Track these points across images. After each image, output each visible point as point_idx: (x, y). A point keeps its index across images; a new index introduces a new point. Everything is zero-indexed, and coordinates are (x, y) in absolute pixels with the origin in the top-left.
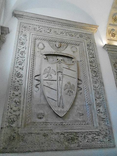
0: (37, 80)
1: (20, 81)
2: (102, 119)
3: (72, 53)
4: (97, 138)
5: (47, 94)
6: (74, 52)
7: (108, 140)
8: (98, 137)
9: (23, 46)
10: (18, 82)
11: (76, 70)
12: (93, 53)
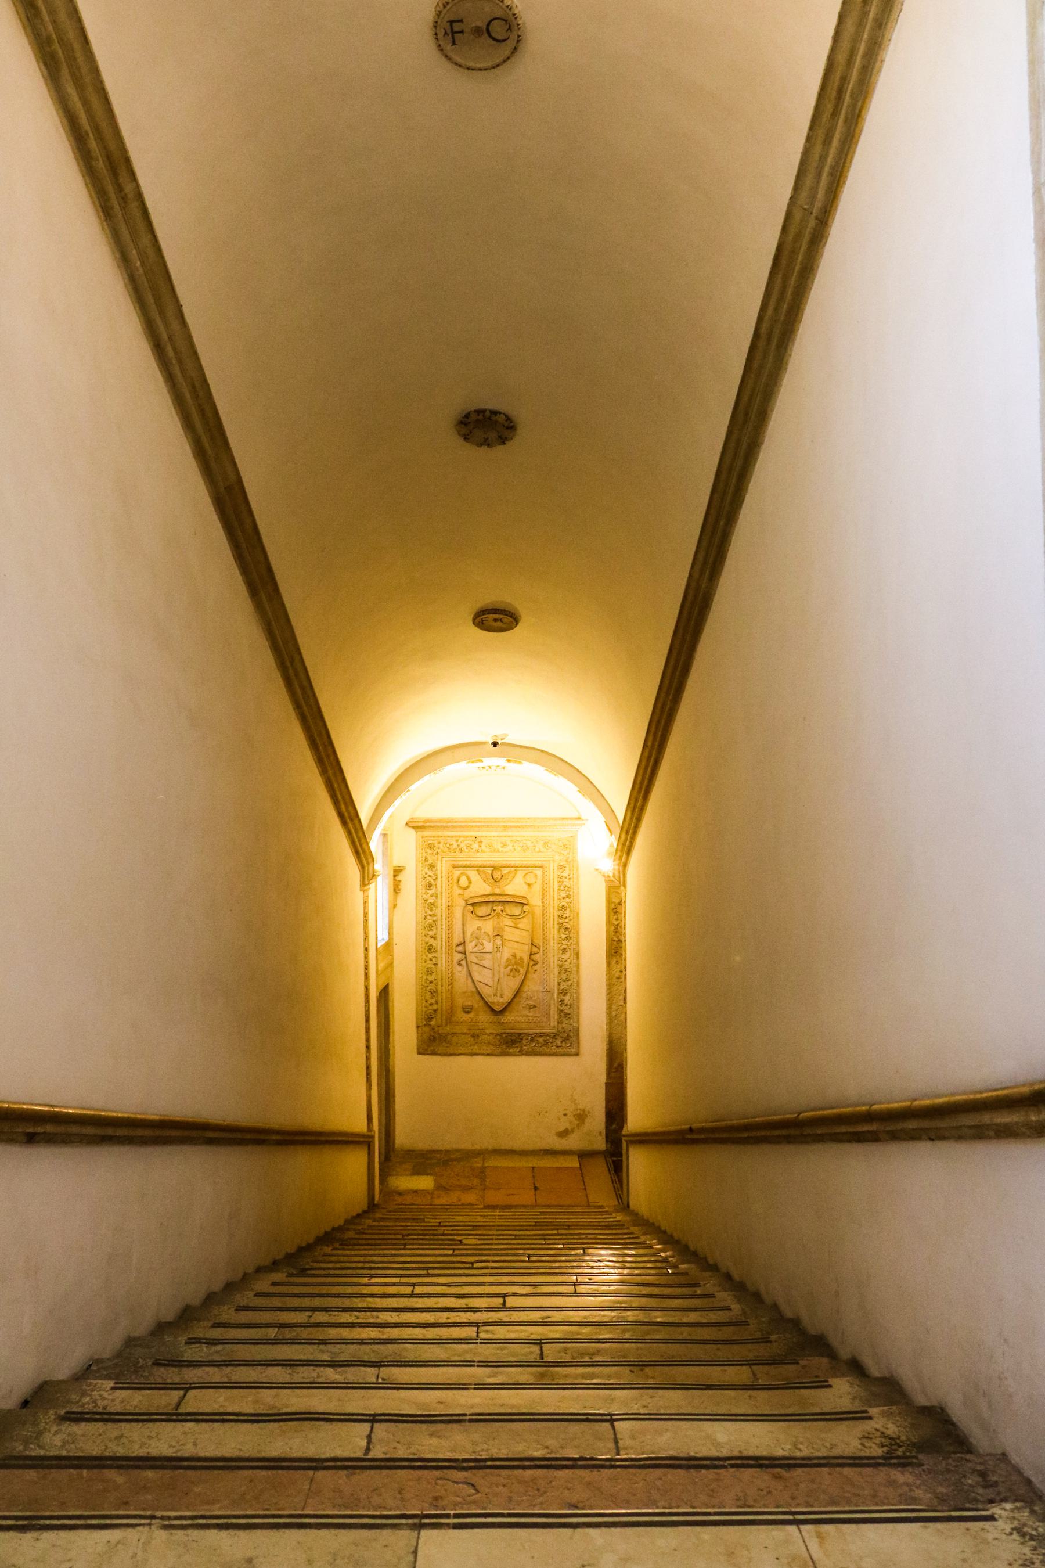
3: (526, 887)
5: (477, 977)
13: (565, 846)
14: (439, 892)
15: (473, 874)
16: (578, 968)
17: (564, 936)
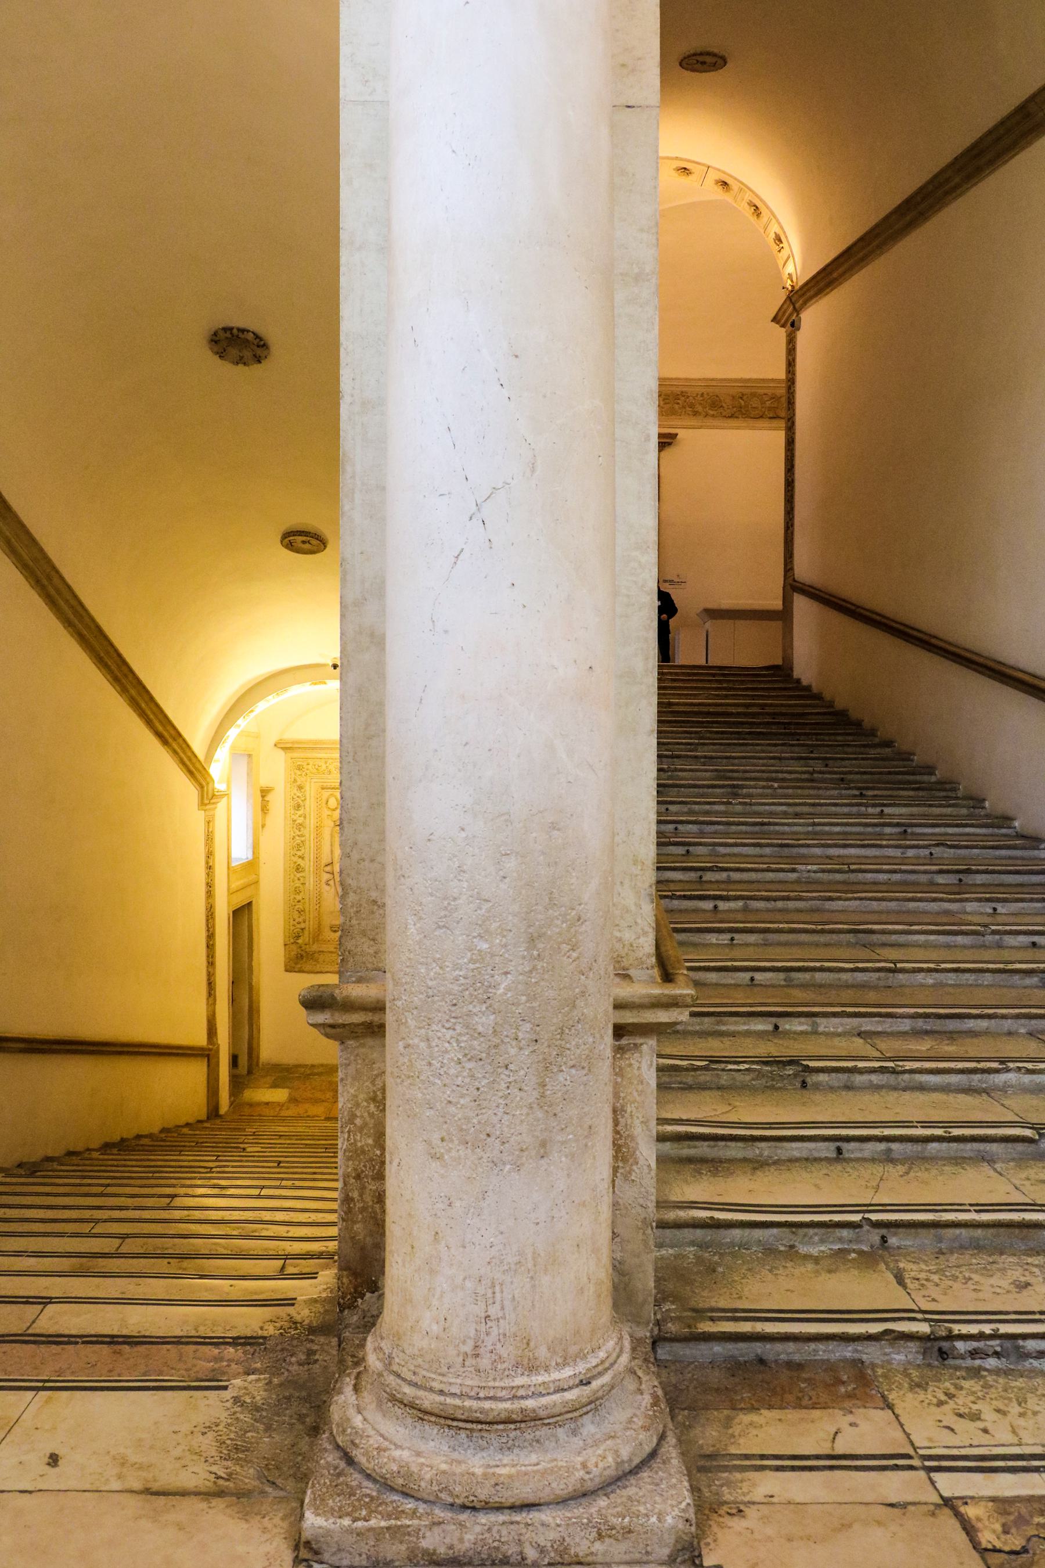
9: (300, 813)
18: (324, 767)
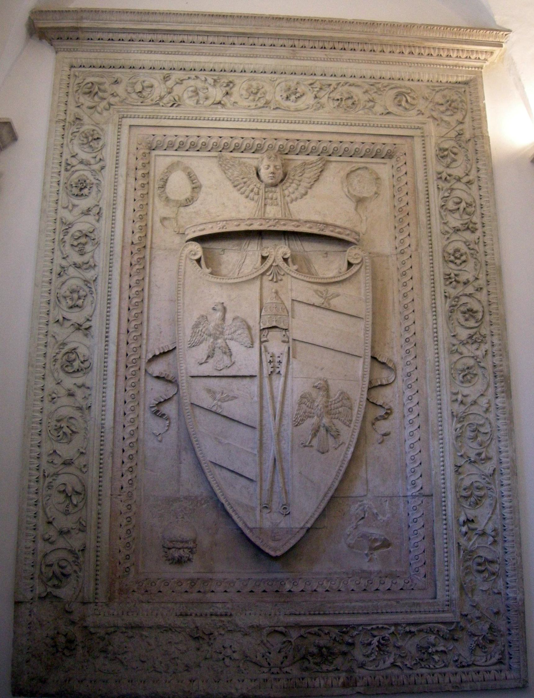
0: (158, 377)
1: (79, 393)
2: (479, 564)
3: (350, 205)
4: (442, 648)
5: (209, 451)
6: (360, 201)
7: (494, 660)
8: (451, 645)
9: (84, 204)
10: (71, 395)
11: (364, 308)
12: (469, 200)
13: (451, 106)
14: (103, 204)
15: (206, 168)
16: (510, 419)
17: (464, 334)
18: (160, 89)
